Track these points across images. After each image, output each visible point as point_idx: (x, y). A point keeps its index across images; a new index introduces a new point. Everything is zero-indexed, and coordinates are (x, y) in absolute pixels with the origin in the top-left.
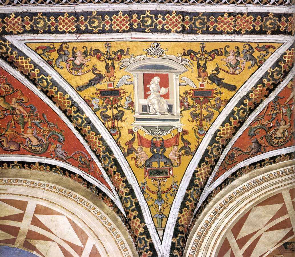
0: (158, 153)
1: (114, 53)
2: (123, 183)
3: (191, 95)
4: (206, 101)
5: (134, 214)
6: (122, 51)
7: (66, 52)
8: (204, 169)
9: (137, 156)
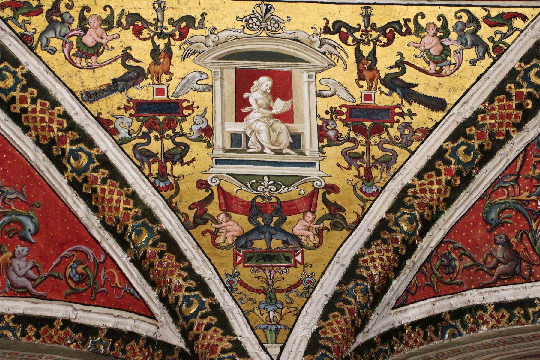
0: (267, 225)
1: (171, 21)
2: (183, 273)
3: (344, 117)
4: (378, 129)
5: (206, 321)
6: (190, 19)
7: (67, 17)
8: (379, 252)
9: (217, 230)
